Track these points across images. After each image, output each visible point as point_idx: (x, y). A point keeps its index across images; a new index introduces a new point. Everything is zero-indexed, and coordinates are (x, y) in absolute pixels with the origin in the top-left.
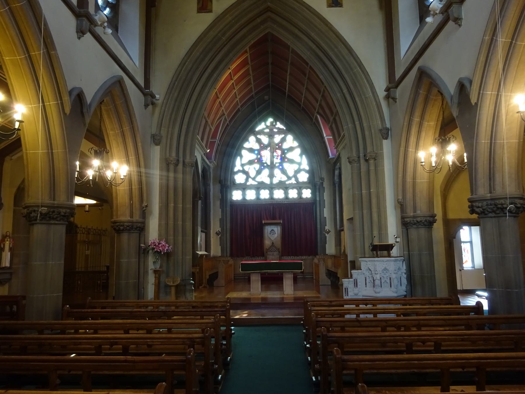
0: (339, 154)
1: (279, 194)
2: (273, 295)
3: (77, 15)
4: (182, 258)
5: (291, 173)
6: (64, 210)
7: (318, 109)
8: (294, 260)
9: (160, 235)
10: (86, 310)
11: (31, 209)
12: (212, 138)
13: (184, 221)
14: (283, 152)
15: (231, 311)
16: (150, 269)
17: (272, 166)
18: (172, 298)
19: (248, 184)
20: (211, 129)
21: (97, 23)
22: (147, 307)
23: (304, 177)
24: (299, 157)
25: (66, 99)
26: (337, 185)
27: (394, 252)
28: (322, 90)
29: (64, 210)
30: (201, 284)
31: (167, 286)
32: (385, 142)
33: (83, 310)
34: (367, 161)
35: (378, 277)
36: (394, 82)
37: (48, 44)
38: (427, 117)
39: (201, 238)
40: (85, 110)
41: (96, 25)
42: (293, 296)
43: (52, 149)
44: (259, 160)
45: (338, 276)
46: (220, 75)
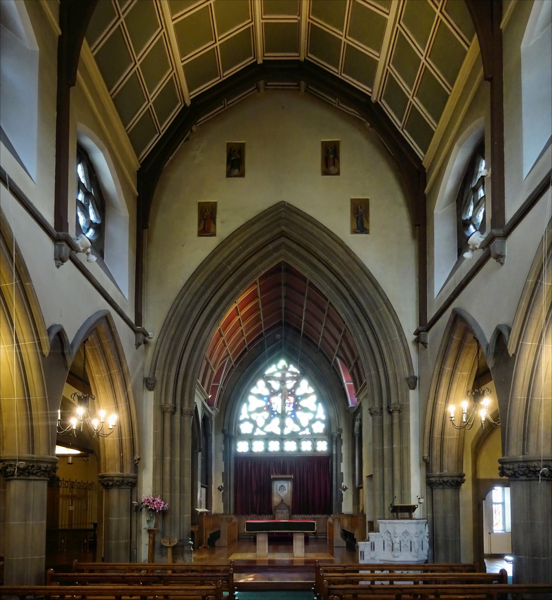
0: (361, 403)
1: (290, 447)
2: (281, 557)
3: (56, 240)
4: (180, 517)
5: (305, 423)
6: (45, 465)
7: (338, 351)
8: (305, 519)
9: (154, 491)
10: (72, 574)
11: (7, 463)
12: (214, 382)
13: (182, 475)
14: (297, 399)
15: (235, 575)
16: (143, 527)
17: (282, 414)
18: (168, 560)
19: (255, 434)
20: (213, 372)
21: (79, 249)
22: (139, 570)
23: (319, 428)
24: (315, 405)
25: (44, 338)
26: (357, 438)
27: (417, 514)
28: (343, 330)
29: (45, 465)
30: (200, 544)
31: (162, 547)
32: (411, 392)
33: (69, 574)
34: (390, 413)
35: (398, 540)
36: (425, 325)
37: (22, 274)
38: (460, 366)
39: (201, 494)
40: (66, 351)
41: (78, 251)
42: (303, 559)
43: (29, 396)
44: (269, 408)
45: (355, 537)
46: (224, 310)
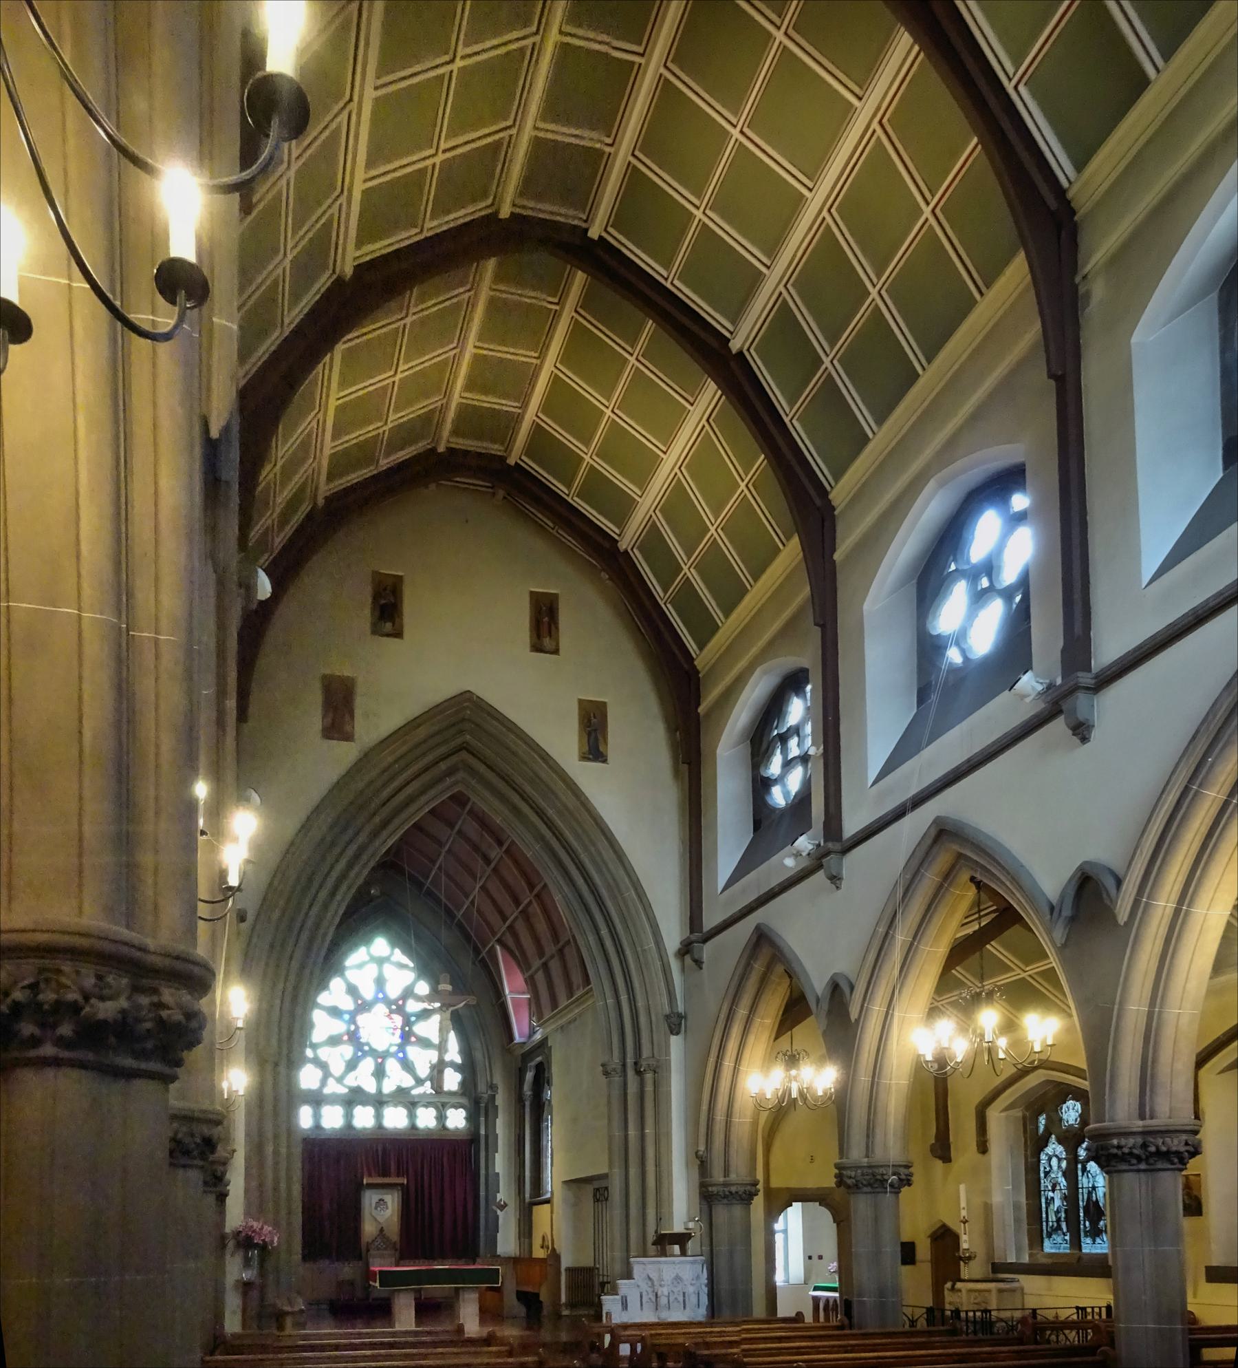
19: (327, 1091)
